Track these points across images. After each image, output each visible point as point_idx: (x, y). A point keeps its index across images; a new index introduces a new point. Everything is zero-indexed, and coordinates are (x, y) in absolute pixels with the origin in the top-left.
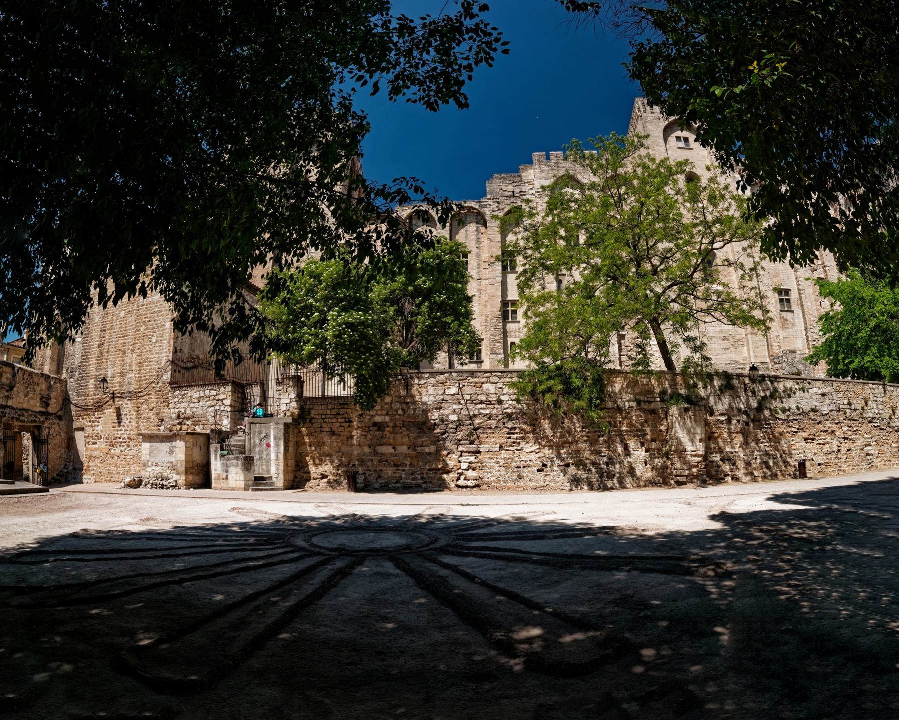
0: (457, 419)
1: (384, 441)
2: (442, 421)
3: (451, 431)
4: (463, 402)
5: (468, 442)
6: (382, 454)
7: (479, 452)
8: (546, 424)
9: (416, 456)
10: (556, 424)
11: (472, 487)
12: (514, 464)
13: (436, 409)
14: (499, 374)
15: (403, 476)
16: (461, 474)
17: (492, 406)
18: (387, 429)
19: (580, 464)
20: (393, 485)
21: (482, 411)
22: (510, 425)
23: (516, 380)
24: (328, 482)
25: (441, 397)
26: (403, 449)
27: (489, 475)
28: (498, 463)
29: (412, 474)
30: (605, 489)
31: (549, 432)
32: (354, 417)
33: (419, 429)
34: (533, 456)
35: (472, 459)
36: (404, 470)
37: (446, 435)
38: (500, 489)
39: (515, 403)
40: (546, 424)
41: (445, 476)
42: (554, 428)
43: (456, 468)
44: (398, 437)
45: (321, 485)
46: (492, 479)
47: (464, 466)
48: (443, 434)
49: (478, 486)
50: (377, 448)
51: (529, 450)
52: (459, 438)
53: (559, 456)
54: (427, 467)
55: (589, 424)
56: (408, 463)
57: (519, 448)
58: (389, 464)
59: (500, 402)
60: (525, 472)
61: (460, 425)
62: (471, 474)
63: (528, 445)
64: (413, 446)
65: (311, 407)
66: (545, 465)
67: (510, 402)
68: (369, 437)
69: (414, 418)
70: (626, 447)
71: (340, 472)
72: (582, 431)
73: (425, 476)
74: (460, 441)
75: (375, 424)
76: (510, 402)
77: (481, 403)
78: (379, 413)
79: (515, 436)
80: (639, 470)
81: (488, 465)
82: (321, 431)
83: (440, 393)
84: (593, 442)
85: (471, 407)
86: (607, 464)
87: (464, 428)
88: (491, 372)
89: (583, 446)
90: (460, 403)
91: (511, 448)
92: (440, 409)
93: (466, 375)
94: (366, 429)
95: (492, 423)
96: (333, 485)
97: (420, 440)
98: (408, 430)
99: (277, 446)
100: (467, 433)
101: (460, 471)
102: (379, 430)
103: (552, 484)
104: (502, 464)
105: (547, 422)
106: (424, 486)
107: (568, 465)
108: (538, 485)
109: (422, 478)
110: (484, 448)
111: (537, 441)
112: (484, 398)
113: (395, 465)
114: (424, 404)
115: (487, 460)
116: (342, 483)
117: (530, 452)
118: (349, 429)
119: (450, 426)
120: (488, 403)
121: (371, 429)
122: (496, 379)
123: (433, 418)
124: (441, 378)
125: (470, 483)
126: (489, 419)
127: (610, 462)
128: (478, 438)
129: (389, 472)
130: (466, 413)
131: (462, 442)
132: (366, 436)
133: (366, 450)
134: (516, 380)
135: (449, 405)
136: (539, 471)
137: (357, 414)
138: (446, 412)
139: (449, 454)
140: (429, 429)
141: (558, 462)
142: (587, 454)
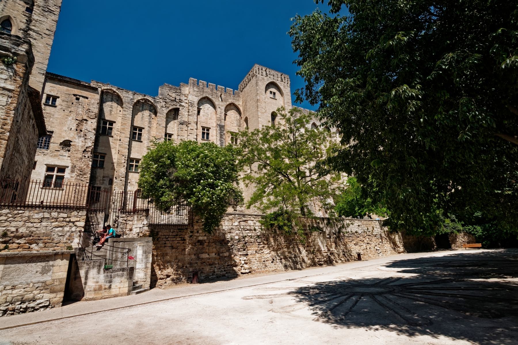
0: (238, 238)
1: (204, 250)
2: (232, 239)
3: (236, 244)
4: (240, 229)
5: (243, 250)
6: (202, 259)
7: (247, 255)
8: (272, 240)
9: (220, 259)
10: (275, 240)
11: (247, 273)
12: (263, 260)
13: (229, 233)
14: (254, 216)
15: (216, 270)
16: (242, 267)
17: (252, 232)
18: (205, 244)
19: (285, 258)
20: (212, 276)
21: (248, 234)
22: (259, 241)
23: (260, 219)
24: (173, 280)
25: (231, 227)
26: (213, 255)
27: (254, 266)
28: (256, 259)
29: (219, 269)
30: (296, 269)
31: (273, 244)
32: (187, 237)
33: (221, 243)
34: (269, 256)
35: (245, 258)
36: (215, 267)
37: (233, 246)
38: (260, 272)
39: (260, 230)
40: (272, 240)
41: (234, 268)
42: (275, 242)
43: (239, 264)
44: (211, 248)
45: (168, 282)
46: (256, 268)
47: (243, 262)
48: (232, 246)
49: (250, 272)
50: (200, 255)
51: (266, 253)
52: (239, 248)
53: (278, 256)
54: (227, 264)
55: (287, 239)
56: (217, 263)
57: (262, 252)
58: (207, 265)
59: (255, 230)
60: (267, 263)
61: (239, 241)
62: (245, 266)
63: (266, 250)
64: (218, 253)
65: (159, 230)
66: (273, 260)
67: (259, 230)
68: (195, 249)
69: (219, 238)
70: (299, 250)
71: (179, 272)
72: (284, 243)
73: (226, 269)
74: (239, 249)
75: (199, 241)
76: (259, 230)
77: (248, 230)
78: (201, 235)
79: (261, 246)
80: (306, 259)
81: (253, 261)
82: (165, 246)
83: (231, 225)
84: (288, 248)
85: (244, 232)
86: (295, 258)
87: (241, 242)
88: (251, 215)
89: (286, 250)
90: (239, 230)
91: (259, 252)
92: (230, 233)
93: (241, 216)
94: (194, 244)
95: (252, 240)
96: (176, 281)
97: (222, 250)
98: (215, 244)
99: (147, 258)
100: (242, 245)
101: (241, 265)
102: (201, 245)
103: (278, 268)
104: (258, 260)
105: (272, 239)
106: (226, 275)
107: (281, 259)
108: (273, 269)
109: (225, 270)
110: (249, 252)
111: (269, 247)
112: (248, 228)
113: (210, 265)
114: (223, 230)
115: (251, 258)
116: (182, 279)
117: (267, 254)
118: (184, 245)
119: (235, 242)
120: (250, 230)
121: (196, 244)
122: (252, 219)
123: (228, 237)
124: (231, 217)
125: (247, 271)
126: (251, 238)
127: (295, 257)
128: (247, 247)
129: (207, 269)
130: (242, 235)
131: (240, 250)
132: (193, 248)
133: (193, 257)
134: (260, 219)
135: (234, 231)
136: (272, 262)
137: (188, 235)
138: (233, 235)
139: (234, 256)
140: (225, 243)
141: (278, 258)
142: (287, 254)
